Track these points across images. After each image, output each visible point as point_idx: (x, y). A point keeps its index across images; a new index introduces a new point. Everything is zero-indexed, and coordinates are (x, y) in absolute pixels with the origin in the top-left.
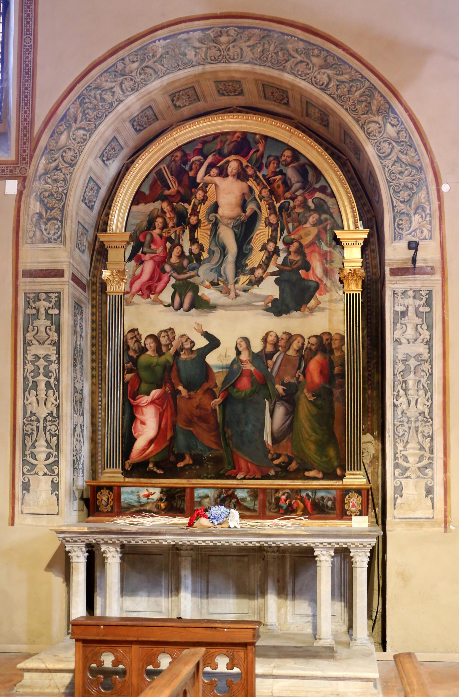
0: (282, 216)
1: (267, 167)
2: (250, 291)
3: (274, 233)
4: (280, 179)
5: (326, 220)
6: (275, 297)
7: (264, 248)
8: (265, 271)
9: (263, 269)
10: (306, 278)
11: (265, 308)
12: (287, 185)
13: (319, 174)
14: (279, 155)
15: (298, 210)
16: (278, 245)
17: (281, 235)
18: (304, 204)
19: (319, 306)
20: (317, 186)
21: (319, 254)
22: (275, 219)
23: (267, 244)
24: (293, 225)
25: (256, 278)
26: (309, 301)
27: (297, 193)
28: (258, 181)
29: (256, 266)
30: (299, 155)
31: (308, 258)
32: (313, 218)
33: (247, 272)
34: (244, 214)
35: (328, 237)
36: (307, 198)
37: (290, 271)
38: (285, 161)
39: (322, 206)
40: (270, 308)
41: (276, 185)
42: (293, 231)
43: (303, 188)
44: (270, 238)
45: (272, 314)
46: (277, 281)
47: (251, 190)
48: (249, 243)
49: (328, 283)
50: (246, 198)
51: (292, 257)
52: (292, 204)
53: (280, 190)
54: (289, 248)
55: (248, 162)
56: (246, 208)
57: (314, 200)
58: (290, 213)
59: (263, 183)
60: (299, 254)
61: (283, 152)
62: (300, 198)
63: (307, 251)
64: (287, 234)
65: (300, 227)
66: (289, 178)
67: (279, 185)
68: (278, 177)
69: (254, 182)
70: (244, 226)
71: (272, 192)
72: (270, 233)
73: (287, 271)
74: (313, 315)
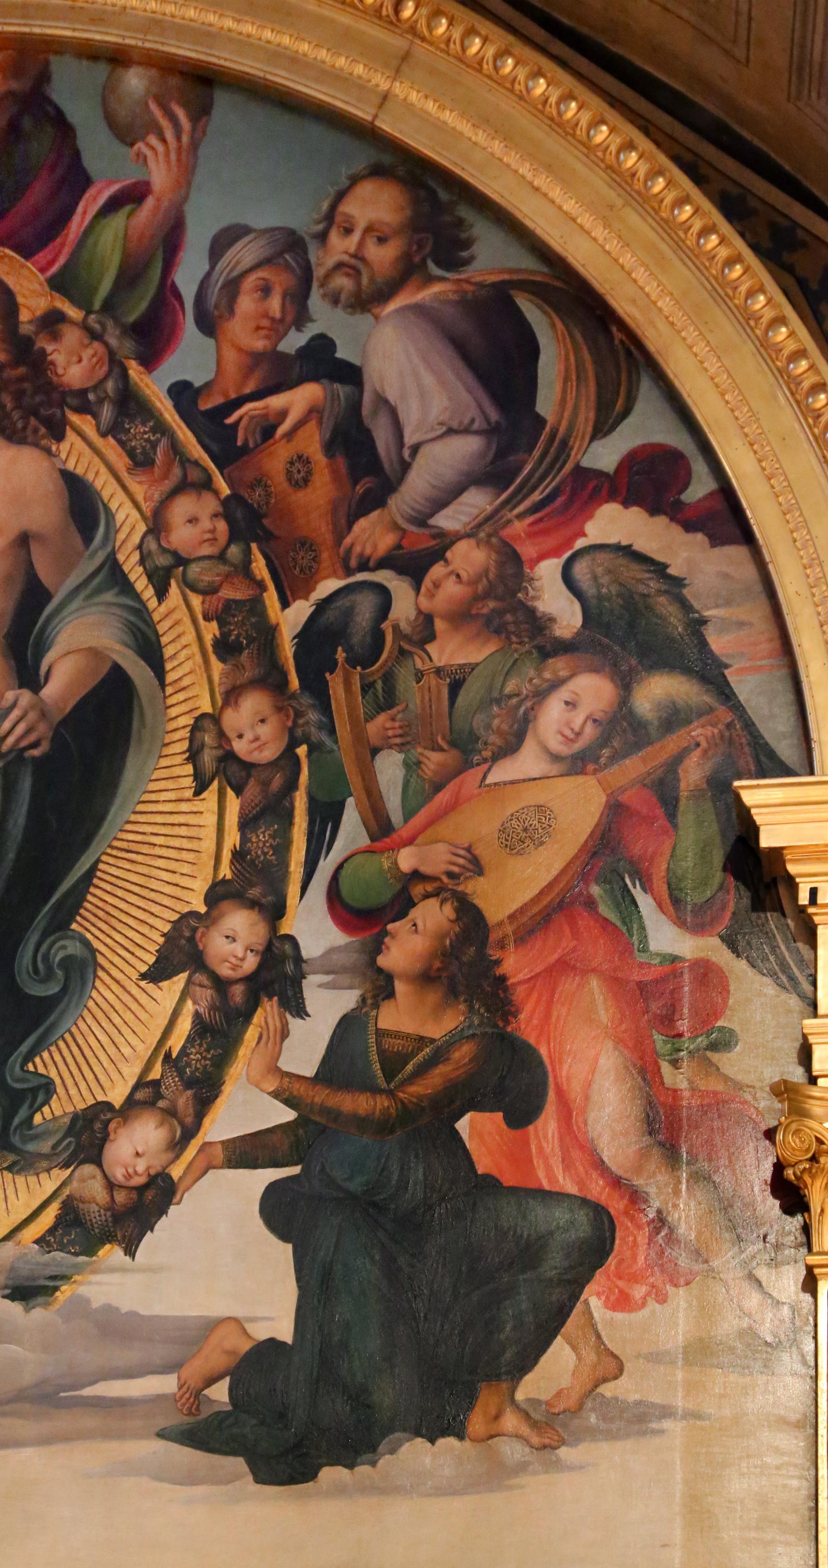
0: (324, 704)
1: (208, 324)
2: (65, 1292)
3: (262, 837)
4: (313, 412)
5: (674, 718)
6: (261, 1332)
7: (180, 954)
8: (189, 1134)
9: (171, 1112)
10: (508, 1180)
11: (175, 1419)
12: (364, 460)
13: (621, 358)
14: (301, 219)
15: (450, 650)
16: (287, 927)
17: (317, 846)
18: (503, 610)
19: (607, 1390)
20: (606, 455)
21: (615, 983)
22: (265, 731)
23: (208, 919)
24: (412, 767)
25: (111, 1186)
26: (526, 1362)
27: (447, 520)
28: (139, 431)
29: (117, 1096)
30: (465, 212)
31: (526, 1025)
32: (577, 701)
33: (45, 1146)
34: (26, 697)
35: (691, 846)
36: (527, 550)
37: (382, 1127)
38: (352, 266)
39: (635, 608)
40: (220, 1418)
41: (276, 461)
42: (408, 815)
43: (494, 474)
44: (225, 871)
45: (238, 1464)
46: (277, 1210)
47: (82, 506)
48: (61, 923)
49: (687, 1212)
50: (45, 573)
51: (401, 1016)
52: (405, 605)
53: (318, 497)
54: (377, 947)
55: (59, 284)
56: (41, 648)
57: (581, 570)
58: (389, 678)
59: (175, 448)
60: (452, 993)
61: (341, 196)
62: (469, 557)
63: (515, 965)
64: (364, 841)
65: (472, 777)
66: (382, 401)
67: (302, 459)
68: (299, 399)
69: (110, 448)
70: (26, 784)
71: (246, 520)
72: (233, 838)
73: (361, 1123)
74: (558, 1466)
